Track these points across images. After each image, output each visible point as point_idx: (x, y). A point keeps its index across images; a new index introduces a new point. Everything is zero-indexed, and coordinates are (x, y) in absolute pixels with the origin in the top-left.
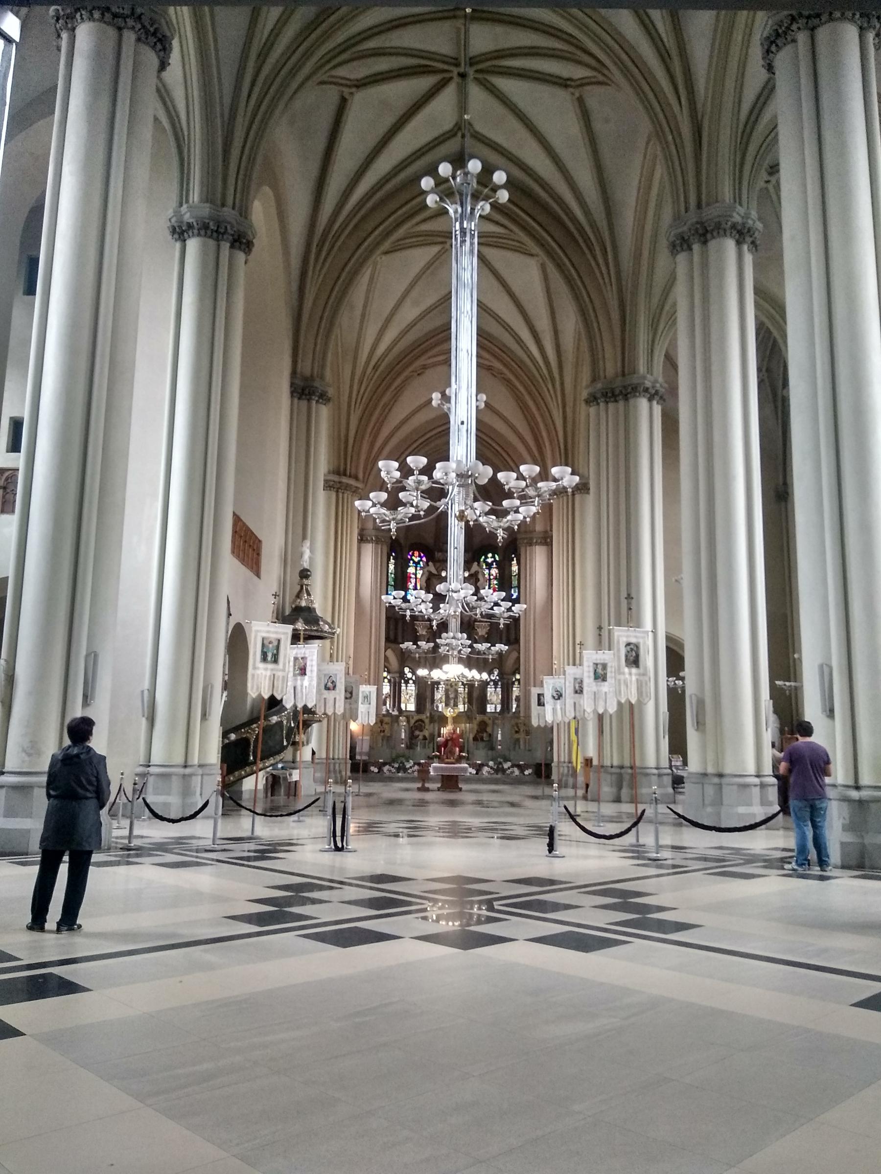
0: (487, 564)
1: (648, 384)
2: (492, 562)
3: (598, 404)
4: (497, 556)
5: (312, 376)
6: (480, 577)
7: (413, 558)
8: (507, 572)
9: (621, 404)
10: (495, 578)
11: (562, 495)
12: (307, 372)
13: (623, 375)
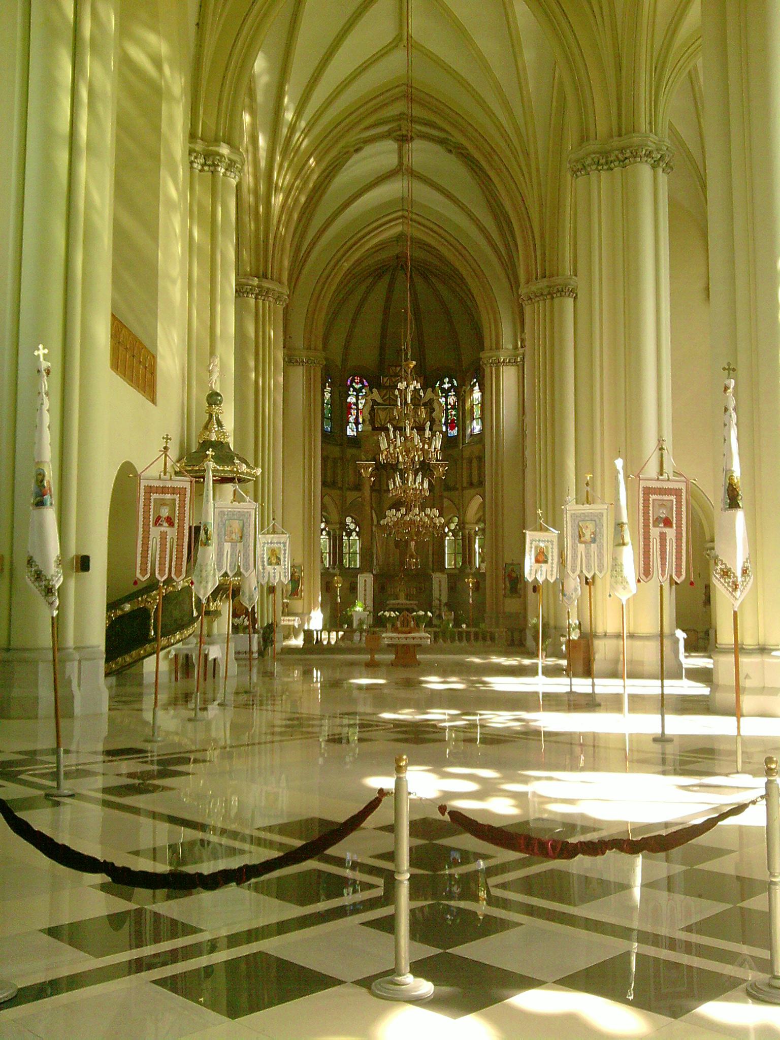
0: (443, 390)
2: (449, 390)
6: (436, 406)
7: (354, 384)
10: (453, 408)
11: (537, 299)
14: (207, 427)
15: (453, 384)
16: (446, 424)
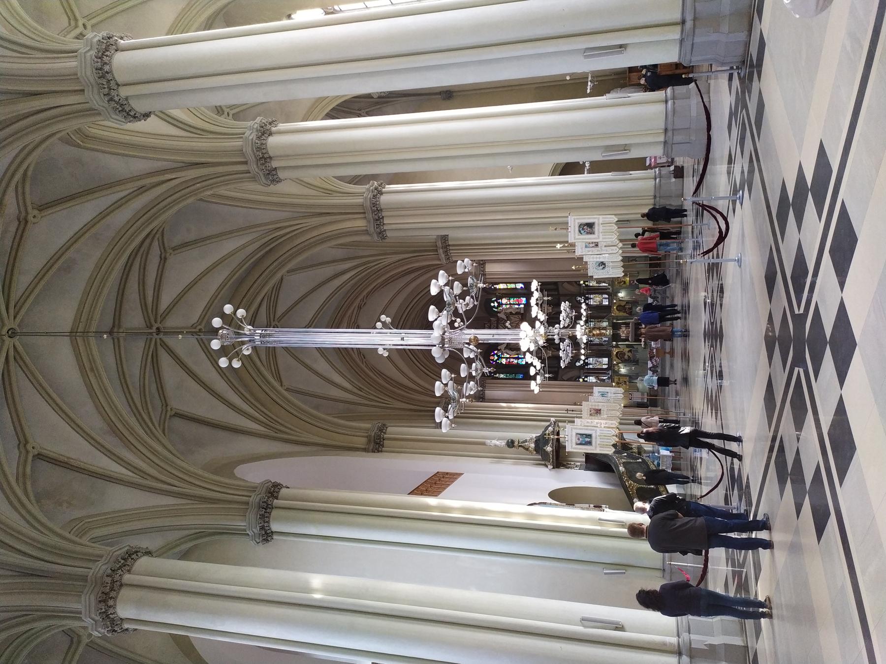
1: (370, 195)
2: (497, 302)
3: (385, 230)
4: (493, 299)
5: (367, 437)
8: (504, 292)
9: (384, 214)
12: (364, 440)
13: (364, 213)
14: (527, 449)
15: (495, 300)
16: (519, 305)
